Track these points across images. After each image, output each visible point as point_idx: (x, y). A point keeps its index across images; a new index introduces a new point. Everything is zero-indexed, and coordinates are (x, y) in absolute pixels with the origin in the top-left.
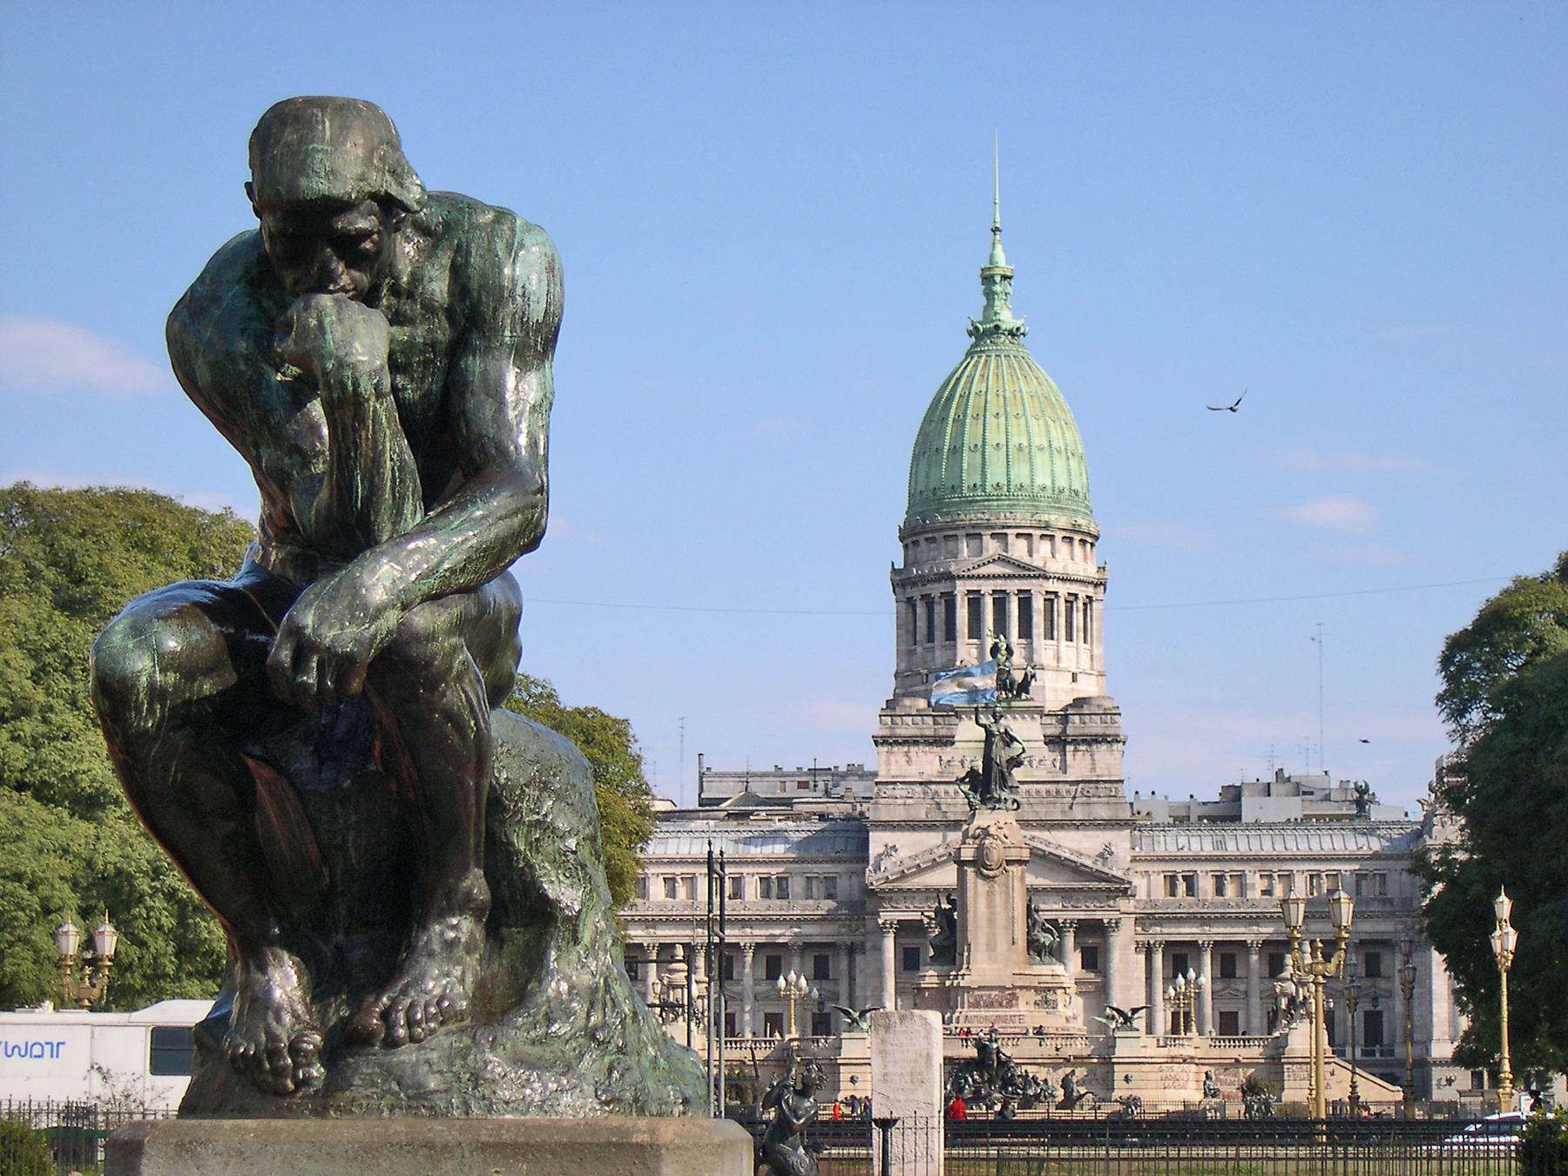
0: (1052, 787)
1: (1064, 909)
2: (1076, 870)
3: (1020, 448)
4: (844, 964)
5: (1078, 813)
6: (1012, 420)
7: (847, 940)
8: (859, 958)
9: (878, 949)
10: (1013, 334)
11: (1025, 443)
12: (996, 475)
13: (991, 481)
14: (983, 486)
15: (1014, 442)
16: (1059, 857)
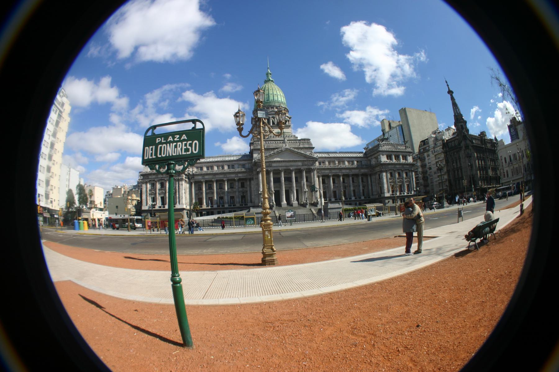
0: (295, 141)
1: (303, 165)
2: (305, 156)
3: (275, 94)
4: (248, 183)
5: (301, 146)
6: (274, 91)
7: (249, 177)
8: (252, 182)
9: (258, 179)
10: (272, 81)
11: (276, 94)
12: (271, 98)
13: (270, 99)
14: (269, 100)
15: (274, 93)
16: (301, 153)
